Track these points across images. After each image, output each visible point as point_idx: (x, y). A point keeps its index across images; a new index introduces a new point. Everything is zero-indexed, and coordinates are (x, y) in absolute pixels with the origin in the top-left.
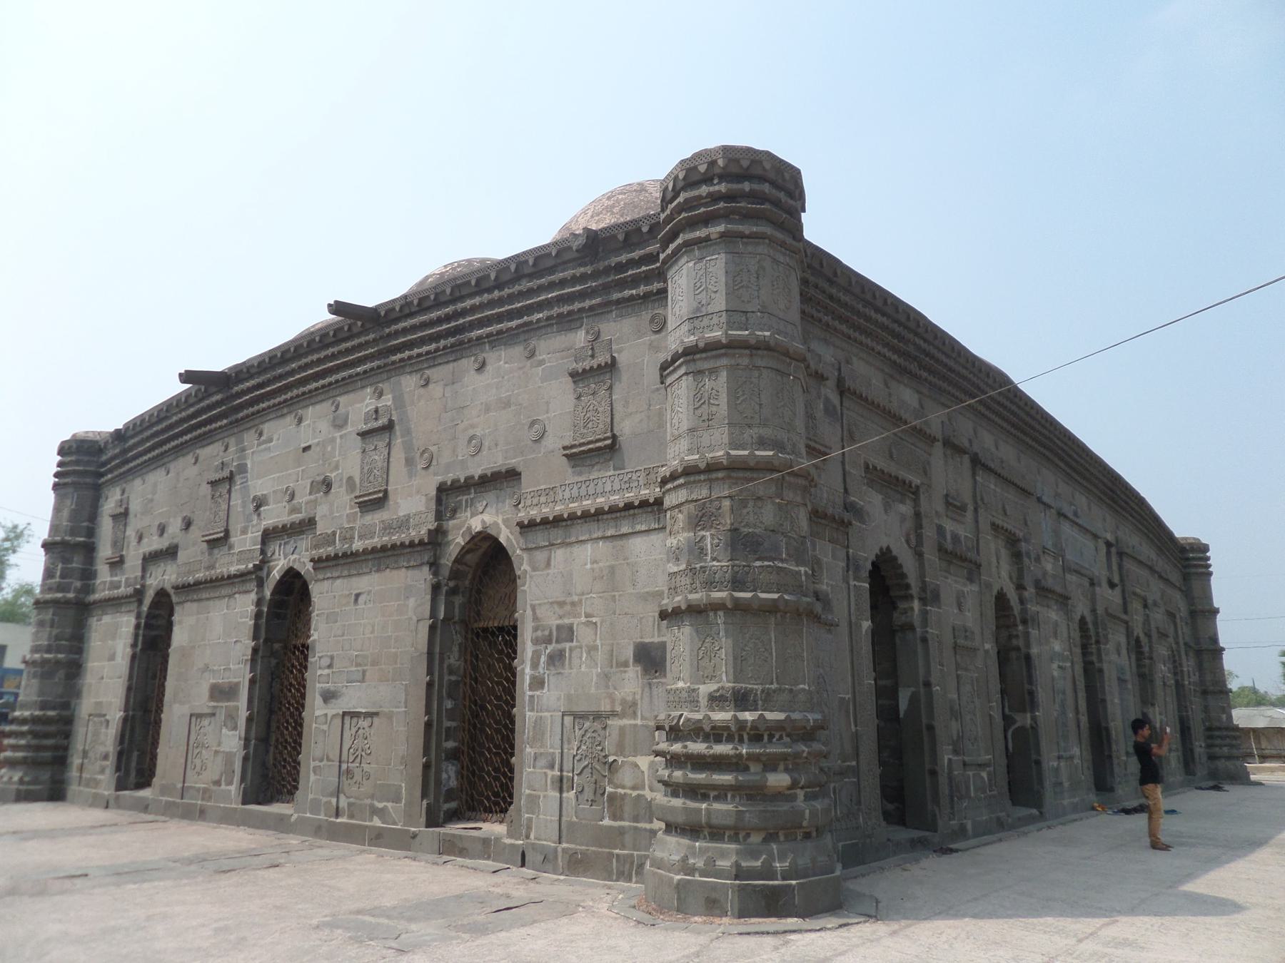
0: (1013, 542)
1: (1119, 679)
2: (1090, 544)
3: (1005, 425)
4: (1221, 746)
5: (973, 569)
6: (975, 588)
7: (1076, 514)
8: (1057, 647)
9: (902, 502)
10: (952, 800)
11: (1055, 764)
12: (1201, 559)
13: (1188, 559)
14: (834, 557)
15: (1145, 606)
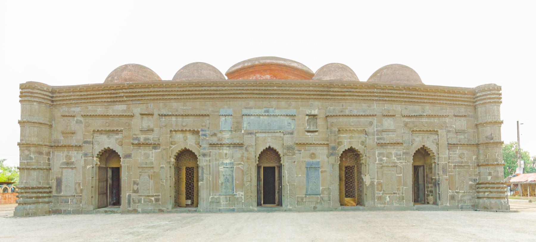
0: (196, 133)
1: (307, 168)
2: (287, 120)
3: (194, 96)
4: (485, 192)
5: (155, 146)
6: (159, 150)
7: (268, 112)
8: (228, 161)
9: (117, 134)
10: (129, 203)
11: (215, 197)
12: (498, 94)
13: (477, 97)
14: (77, 153)
15: (366, 134)
